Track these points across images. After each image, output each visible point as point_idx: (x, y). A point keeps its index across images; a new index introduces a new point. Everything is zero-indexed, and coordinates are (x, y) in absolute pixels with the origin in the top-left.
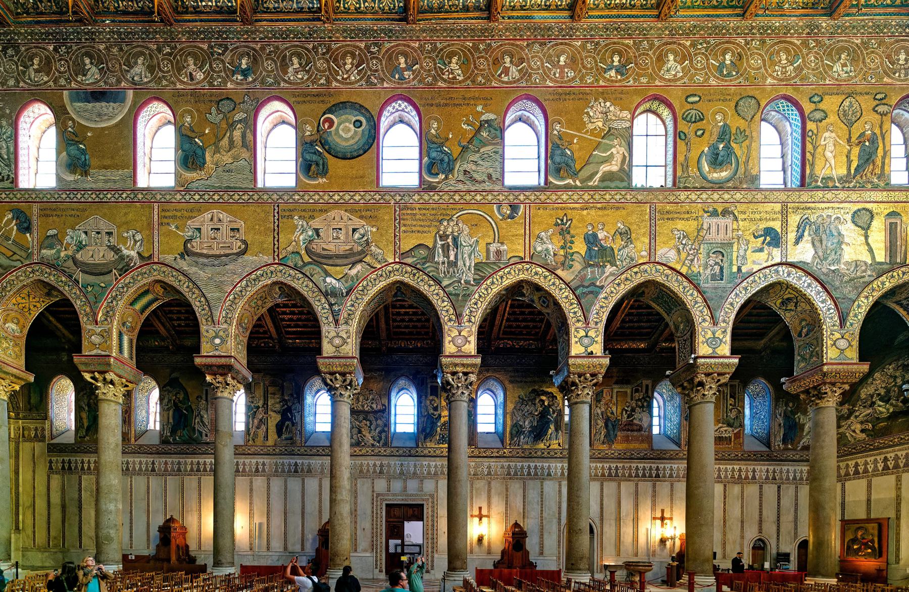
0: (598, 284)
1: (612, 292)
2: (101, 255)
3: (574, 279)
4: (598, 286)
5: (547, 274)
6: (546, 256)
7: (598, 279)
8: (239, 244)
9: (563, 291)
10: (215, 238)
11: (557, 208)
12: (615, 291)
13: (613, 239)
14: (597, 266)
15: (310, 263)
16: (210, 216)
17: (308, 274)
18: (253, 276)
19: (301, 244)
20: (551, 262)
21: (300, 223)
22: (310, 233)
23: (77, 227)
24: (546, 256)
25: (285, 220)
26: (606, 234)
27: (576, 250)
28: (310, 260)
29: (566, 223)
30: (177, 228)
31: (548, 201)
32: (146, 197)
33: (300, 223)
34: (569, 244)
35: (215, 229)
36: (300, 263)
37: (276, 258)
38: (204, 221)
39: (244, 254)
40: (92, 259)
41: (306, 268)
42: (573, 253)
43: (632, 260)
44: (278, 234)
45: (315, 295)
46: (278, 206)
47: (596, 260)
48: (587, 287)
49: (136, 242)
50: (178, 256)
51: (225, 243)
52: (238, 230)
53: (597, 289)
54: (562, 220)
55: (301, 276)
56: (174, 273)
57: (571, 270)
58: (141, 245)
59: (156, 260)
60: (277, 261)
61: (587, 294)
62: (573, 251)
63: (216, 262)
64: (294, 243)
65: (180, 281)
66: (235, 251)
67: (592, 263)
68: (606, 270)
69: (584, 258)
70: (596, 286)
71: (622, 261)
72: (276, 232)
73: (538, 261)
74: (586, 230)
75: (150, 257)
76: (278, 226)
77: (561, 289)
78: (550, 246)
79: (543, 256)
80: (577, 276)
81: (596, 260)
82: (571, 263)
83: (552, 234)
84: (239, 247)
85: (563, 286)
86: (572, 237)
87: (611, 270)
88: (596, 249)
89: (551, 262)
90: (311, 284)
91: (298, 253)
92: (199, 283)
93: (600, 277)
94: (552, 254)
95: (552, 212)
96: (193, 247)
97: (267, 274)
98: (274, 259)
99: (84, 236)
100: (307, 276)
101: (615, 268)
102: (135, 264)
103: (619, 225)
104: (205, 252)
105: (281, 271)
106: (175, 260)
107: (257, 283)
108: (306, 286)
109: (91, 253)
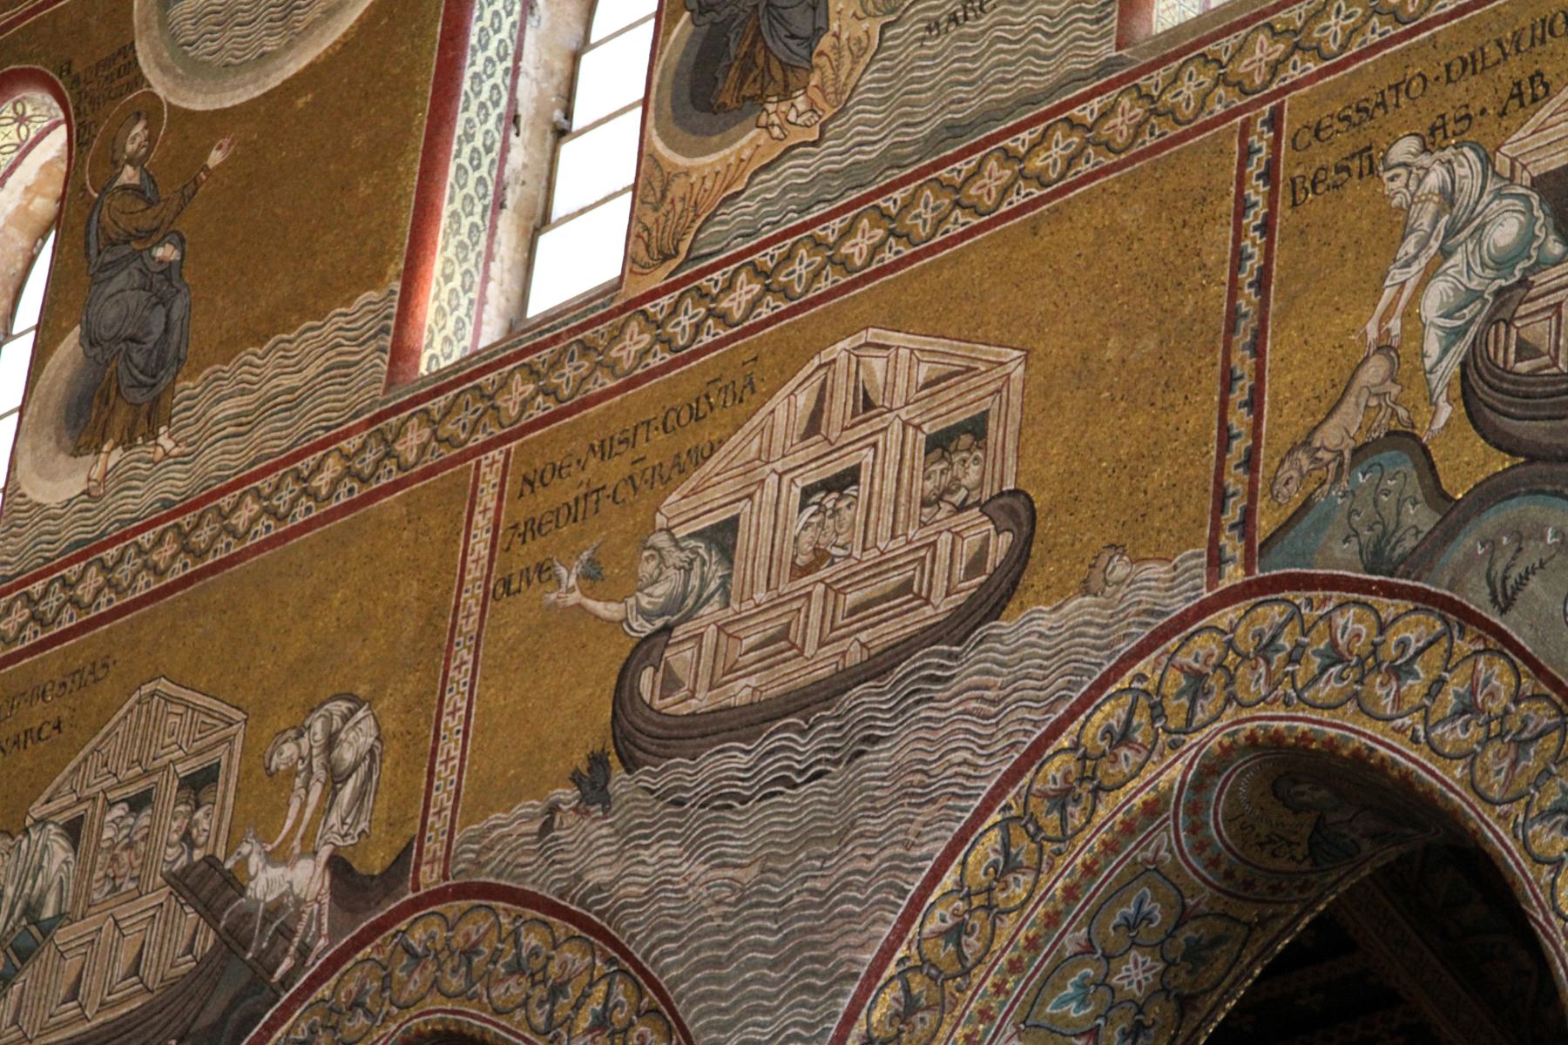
2: (125, 958)
8: (976, 529)
10: (821, 556)
15: (1491, 492)
16: (804, 401)
17: (1477, 599)
18: (1056, 768)
19: (1433, 347)
21: (1433, 180)
22: (1505, 232)
23: (37, 810)
25: (1315, 206)
28: (1500, 462)
30: (592, 577)
32: (449, 428)
33: (1433, 180)
35: (827, 486)
36: (1420, 518)
37: (1232, 545)
38: (764, 455)
39: (995, 613)
40: (71, 1009)
41: (1469, 542)
44: (1257, 349)
45: (1532, 763)
46: (1274, 121)
49: (336, 778)
50: (567, 794)
51: (879, 568)
52: (977, 428)
55: (1415, 629)
56: (531, 940)
58: (360, 796)
59: (430, 877)
60: (1234, 575)
63: (807, 748)
64: (1375, 370)
65: (557, 991)
66: (942, 606)
72: (1243, 337)
75: (401, 865)
76: (1262, 284)
84: (976, 565)
90: (1499, 676)
91: (1404, 439)
92: (671, 967)
96: (670, 683)
97: (1157, 711)
98: (1216, 561)
99: (59, 850)
100: (1468, 616)
102: (304, 952)
104: (740, 692)
105: (1266, 649)
106: (547, 827)
107: (1076, 817)
108: (1468, 708)
109: (72, 965)
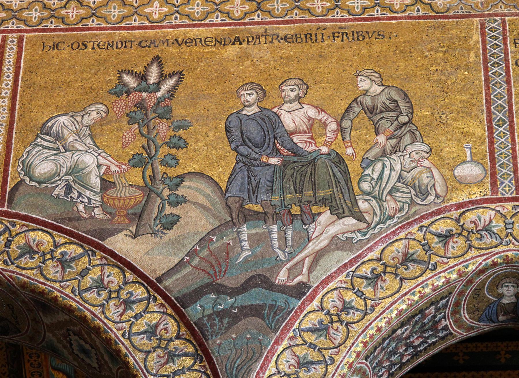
0: (282, 277)
1: (346, 307)
3: (181, 264)
4: (283, 289)
5: (74, 250)
6: (69, 189)
7: (279, 264)
9: (137, 308)
11: (125, 43)
12: (358, 303)
13: (341, 129)
14: (277, 217)
20: (89, 208)
24: (69, 189)
26: (312, 113)
27: (195, 167)
29: (158, 86)
31: (93, 23)
34: (164, 150)
42: (181, 178)
43: (423, 193)
47: (276, 199)
48: (235, 292)
53: (280, 299)
54: (143, 77)
57: (170, 234)
61: (235, 319)
62: (172, 172)
67: (258, 208)
68: (315, 229)
69: (224, 193)
70: (271, 286)
71: (379, 199)
73: (35, 207)
74: (233, 106)
77: (127, 304)
78: (89, 160)
79: (60, 191)
80: (192, 253)
81: (276, 199)
82: (168, 210)
83: (101, 122)
85: (140, 292)
86: (177, 128)
87: (333, 230)
88: (274, 161)
89: (89, 208)
93: (292, 255)
94: (95, 181)
95: (104, 54)
101: (350, 222)
103: (364, 84)
